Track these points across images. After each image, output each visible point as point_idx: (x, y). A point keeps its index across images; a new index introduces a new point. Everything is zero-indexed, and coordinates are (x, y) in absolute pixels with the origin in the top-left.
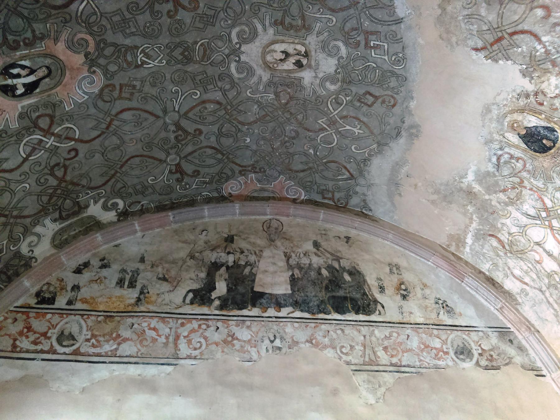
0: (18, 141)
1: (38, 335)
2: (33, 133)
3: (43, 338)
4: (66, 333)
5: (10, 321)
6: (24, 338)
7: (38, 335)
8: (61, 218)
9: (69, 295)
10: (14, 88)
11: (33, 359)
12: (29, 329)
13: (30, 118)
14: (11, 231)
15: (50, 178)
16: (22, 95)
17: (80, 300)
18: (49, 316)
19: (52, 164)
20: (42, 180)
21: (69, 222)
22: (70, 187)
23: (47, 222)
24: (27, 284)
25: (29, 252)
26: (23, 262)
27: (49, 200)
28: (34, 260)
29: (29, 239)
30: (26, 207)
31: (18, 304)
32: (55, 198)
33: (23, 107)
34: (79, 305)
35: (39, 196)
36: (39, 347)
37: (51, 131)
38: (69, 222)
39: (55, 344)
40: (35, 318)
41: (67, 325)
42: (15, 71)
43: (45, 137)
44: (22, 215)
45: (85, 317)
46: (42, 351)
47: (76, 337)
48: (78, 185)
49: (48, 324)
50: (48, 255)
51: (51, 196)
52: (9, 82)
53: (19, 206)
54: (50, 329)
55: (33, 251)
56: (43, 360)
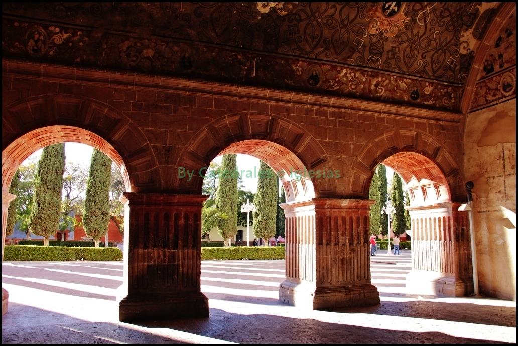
0: (415, 22)
1: (494, 91)
2: (417, 14)
3: (496, 91)
4: (506, 84)
5: (479, 88)
6: (489, 95)
7: (494, 91)
8: (469, 27)
9: (499, 62)
10: (393, 10)
11: (497, 104)
12: (489, 89)
13: (411, 11)
14: (449, 51)
15: (445, 19)
16: (398, 9)
17: (506, 62)
18: (494, 78)
19: (439, 14)
20: (442, 23)
21: (475, 23)
22: (458, 13)
23: (463, 33)
24: (477, 66)
25: (467, 51)
26: (469, 57)
27: (454, 25)
28: (473, 53)
29: (462, 47)
30: (446, 38)
31: (478, 79)
32: (456, 23)
33: (403, 12)
34: (506, 66)
35: (447, 29)
36: (497, 97)
37: (424, 5)
38: (475, 23)
39: (503, 92)
40: (489, 82)
41: (505, 79)
42: (387, 6)
43: (424, 10)
44: (447, 42)
45: (512, 70)
46: (499, 98)
47: (512, 84)
48: (462, 8)
49: (496, 83)
50: (478, 45)
51: (453, 24)
52: (389, 10)
53: (442, 40)
54: (498, 85)
55: (469, 49)
56: (501, 102)
